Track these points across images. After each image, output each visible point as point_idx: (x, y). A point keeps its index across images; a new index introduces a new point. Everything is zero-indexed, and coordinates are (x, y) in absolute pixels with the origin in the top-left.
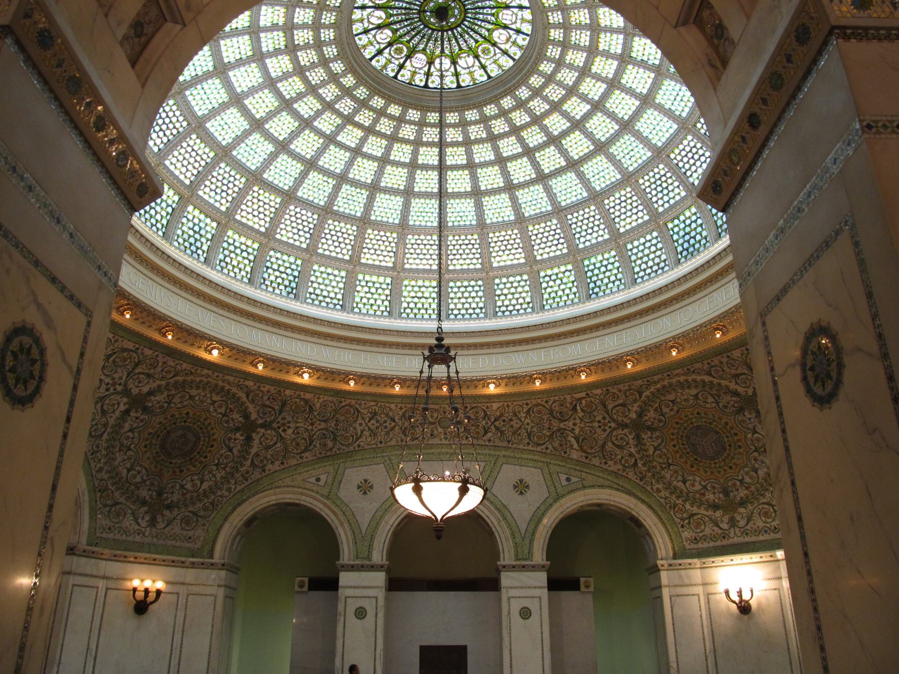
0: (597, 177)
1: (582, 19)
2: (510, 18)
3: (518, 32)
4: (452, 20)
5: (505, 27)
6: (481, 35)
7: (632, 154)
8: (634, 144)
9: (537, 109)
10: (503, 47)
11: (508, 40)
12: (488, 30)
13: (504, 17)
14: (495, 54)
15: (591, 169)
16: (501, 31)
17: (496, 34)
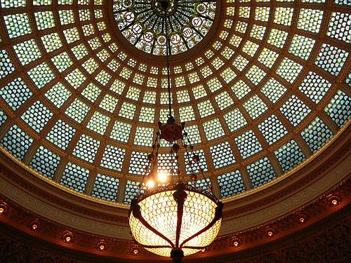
0: (15, 21)
1: (124, 74)
2: (137, 29)
3: (127, 28)
4: (156, 4)
5: (133, 23)
6: (138, 8)
7: (26, 53)
8: (32, 57)
9: (83, 13)
10: (124, 13)
11: (126, 18)
12: (138, 14)
13: (138, 28)
14: (122, 5)
15: (23, 20)
16: (132, 20)
17: (133, 15)
